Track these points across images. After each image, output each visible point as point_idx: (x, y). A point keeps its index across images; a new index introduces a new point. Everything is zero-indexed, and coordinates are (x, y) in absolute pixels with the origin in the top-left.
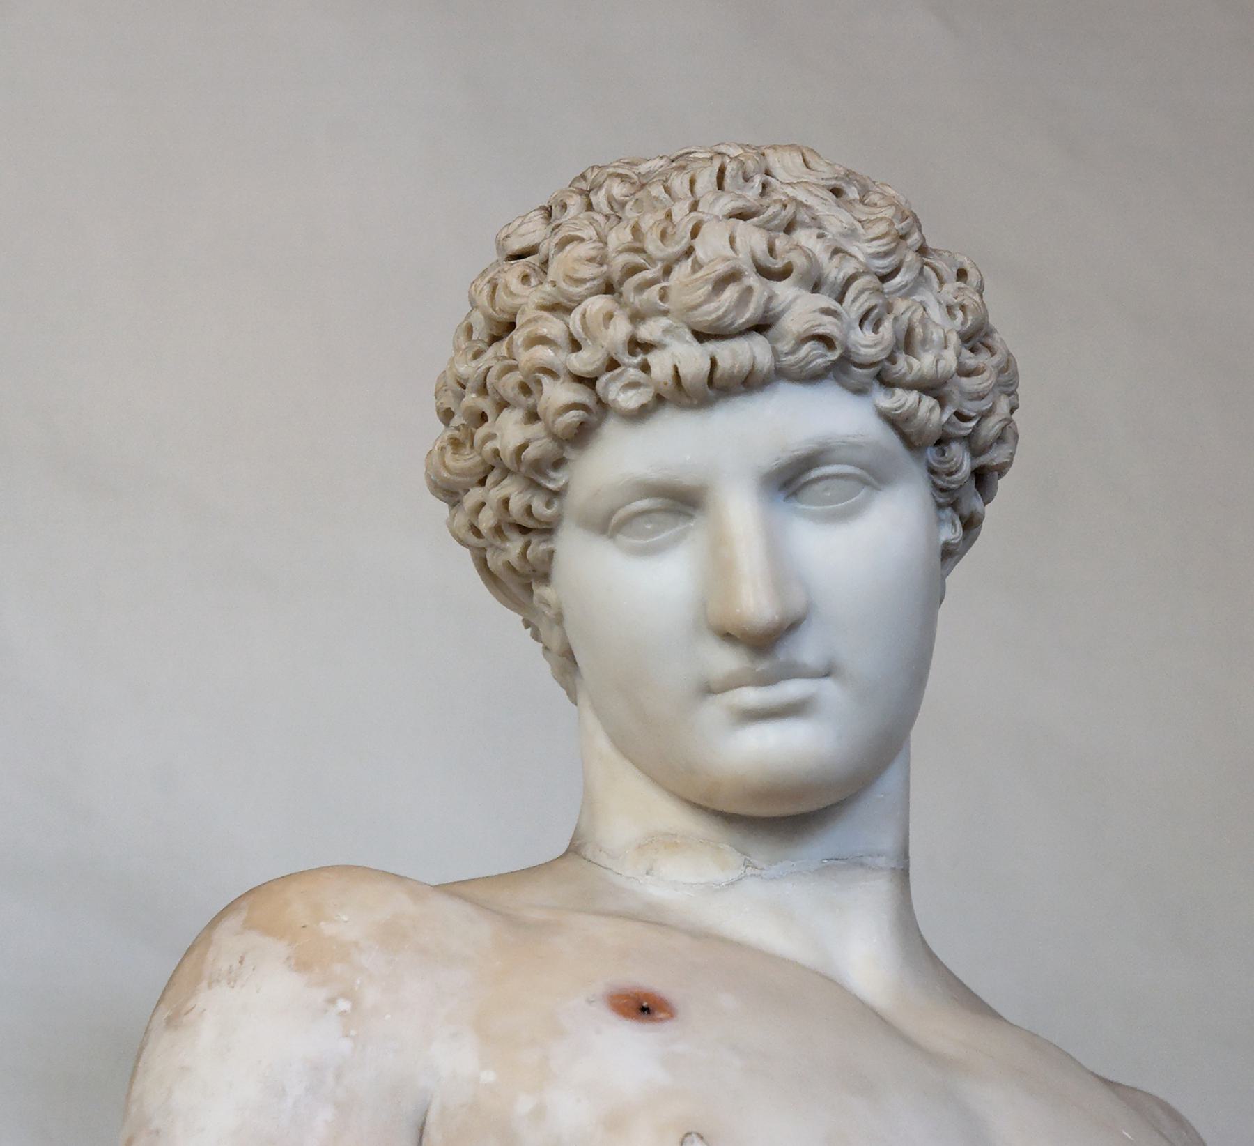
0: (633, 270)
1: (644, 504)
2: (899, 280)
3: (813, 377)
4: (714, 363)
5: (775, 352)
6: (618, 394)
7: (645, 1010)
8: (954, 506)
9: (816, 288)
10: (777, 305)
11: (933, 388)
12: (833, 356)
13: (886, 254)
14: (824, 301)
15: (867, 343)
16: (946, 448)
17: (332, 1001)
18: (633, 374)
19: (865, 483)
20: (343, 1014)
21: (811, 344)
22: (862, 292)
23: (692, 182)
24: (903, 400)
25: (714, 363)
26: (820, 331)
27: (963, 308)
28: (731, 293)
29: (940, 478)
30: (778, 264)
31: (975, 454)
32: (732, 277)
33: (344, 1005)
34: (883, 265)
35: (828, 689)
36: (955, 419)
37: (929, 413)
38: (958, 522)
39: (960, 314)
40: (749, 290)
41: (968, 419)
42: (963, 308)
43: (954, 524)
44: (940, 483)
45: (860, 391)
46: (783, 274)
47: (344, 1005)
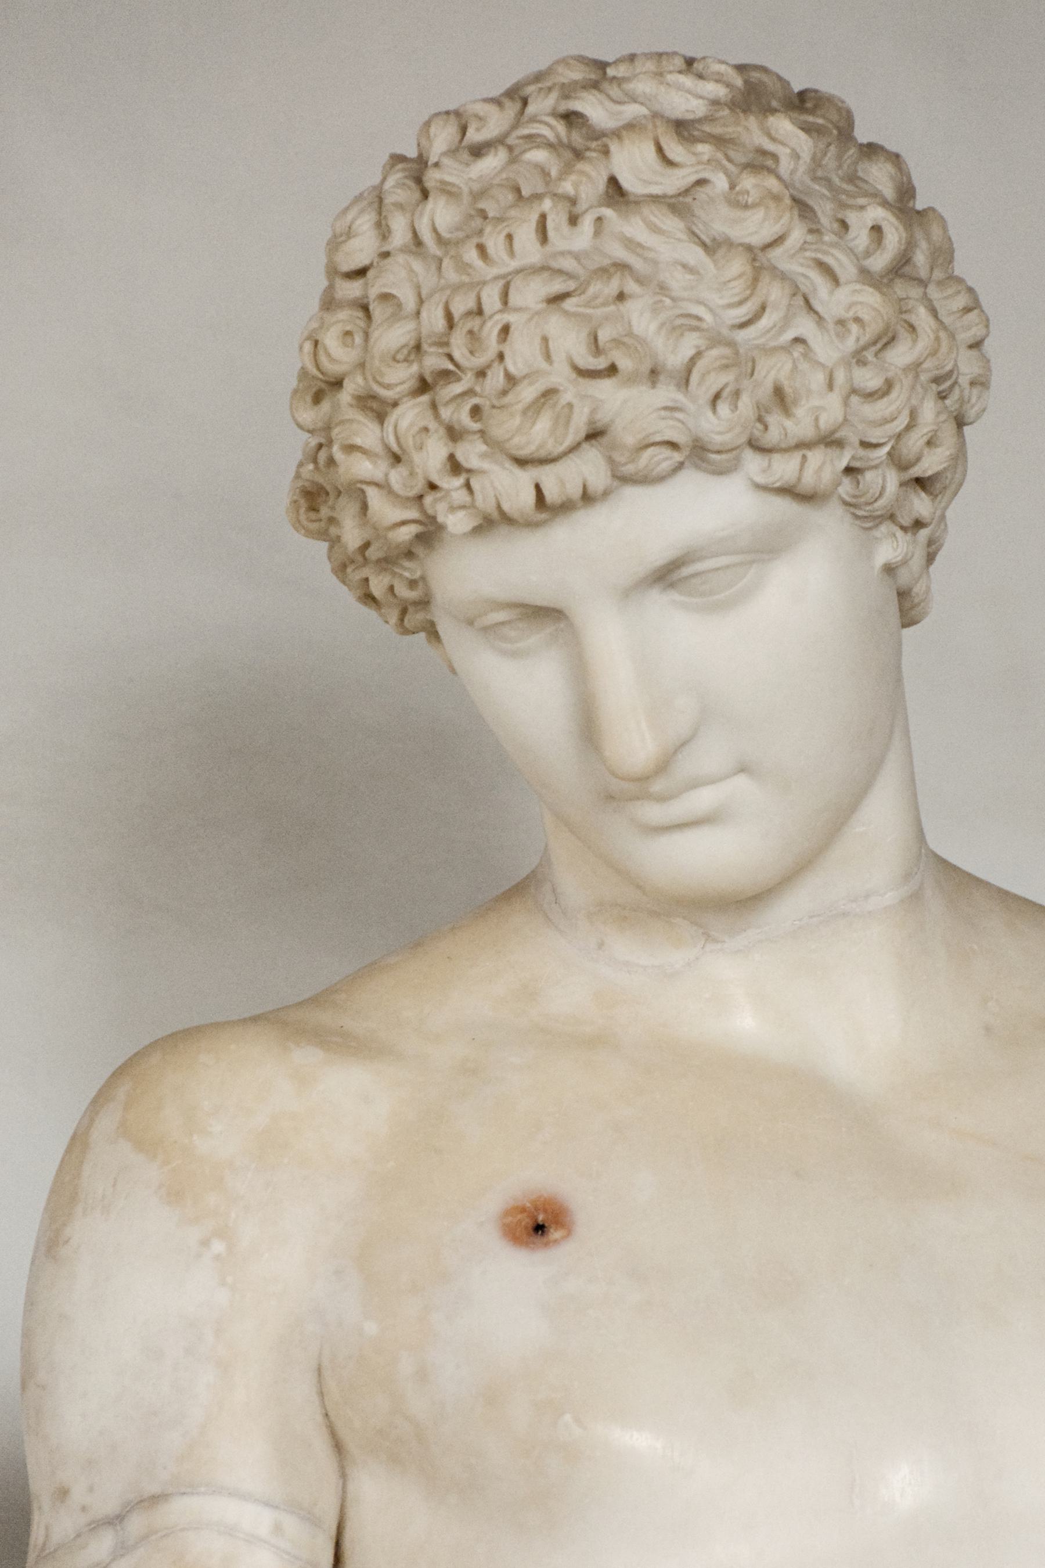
0: (445, 375)
1: (501, 616)
2: (764, 322)
4: (538, 488)
6: (446, 516)
7: (539, 1229)
8: (892, 517)
14: (666, 393)
16: (859, 477)
17: (205, 1243)
18: (460, 496)
19: (752, 562)
20: (217, 1258)
23: (510, 237)
24: (784, 469)
25: (538, 488)
26: (658, 438)
27: (857, 320)
29: (861, 509)
30: (601, 363)
33: (218, 1247)
34: (741, 313)
38: (899, 533)
39: (854, 328)
41: (877, 446)
42: (857, 320)
44: (860, 513)
47: (218, 1247)
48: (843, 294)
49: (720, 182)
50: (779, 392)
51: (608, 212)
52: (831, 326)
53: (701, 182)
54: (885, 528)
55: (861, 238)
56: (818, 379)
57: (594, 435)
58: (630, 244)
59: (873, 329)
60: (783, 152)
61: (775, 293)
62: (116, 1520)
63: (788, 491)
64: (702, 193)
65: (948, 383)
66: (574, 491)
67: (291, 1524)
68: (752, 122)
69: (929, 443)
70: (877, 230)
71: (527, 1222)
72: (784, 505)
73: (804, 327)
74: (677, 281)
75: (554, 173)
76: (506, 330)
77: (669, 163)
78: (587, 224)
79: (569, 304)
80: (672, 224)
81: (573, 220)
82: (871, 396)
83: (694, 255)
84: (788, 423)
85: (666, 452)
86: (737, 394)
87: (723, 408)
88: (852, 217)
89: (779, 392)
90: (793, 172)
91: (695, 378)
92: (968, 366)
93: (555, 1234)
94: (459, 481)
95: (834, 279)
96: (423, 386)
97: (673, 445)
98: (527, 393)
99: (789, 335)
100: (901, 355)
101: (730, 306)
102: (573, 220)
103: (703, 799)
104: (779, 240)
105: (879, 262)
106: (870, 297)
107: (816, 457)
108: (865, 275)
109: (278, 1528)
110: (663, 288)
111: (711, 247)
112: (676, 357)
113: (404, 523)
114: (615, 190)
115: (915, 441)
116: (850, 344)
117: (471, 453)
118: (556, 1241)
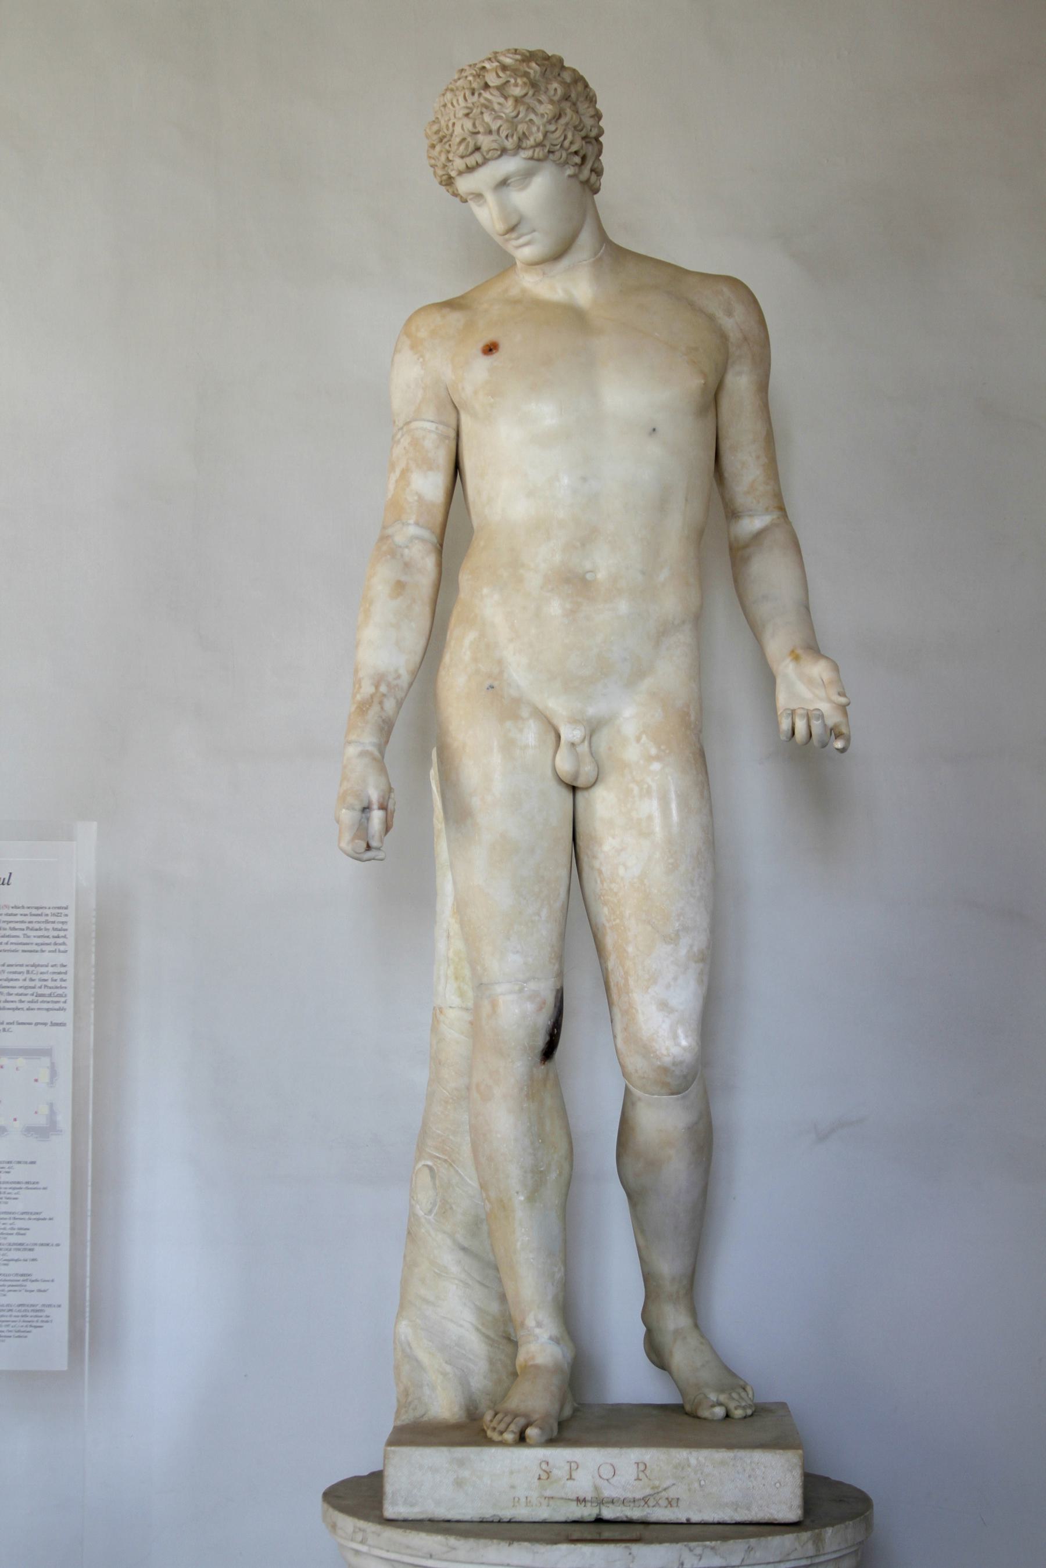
2: (520, 116)
3: (500, 156)
5: (483, 155)
7: (491, 350)
8: (568, 163)
9: (490, 132)
10: (479, 144)
11: (540, 145)
12: (499, 153)
13: (513, 111)
14: (494, 137)
15: (510, 144)
17: (418, 359)
19: (526, 178)
21: (492, 151)
22: (503, 131)
23: (458, 100)
24: (529, 153)
26: (492, 148)
28: (462, 147)
30: (477, 131)
31: (567, 150)
32: (464, 140)
33: (421, 360)
34: (514, 114)
35: (535, 234)
36: (552, 147)
37: (539, 153)
40: (469, 142)
41: (556, 145)
42: (547, 114)
43: (569, 168)
45: (515, 154)
46: (478, 133)
47: (421, 360)
48: (542, 107)
49: (512, 81)
50: (524, 133)
51: (482, 92)
52: (539, 116)
53: (508, 82)
54: (567, 166)
55: (552, 92)
56: (534, 129)
57: (477, 149)
58: (486, 99)
59: (550, 116)
60: (532, 72)
61: (522, 109)
62: (402, 428)
63: (532, 158)
64: (508, 84)
65: (582, 125)
66: (474, 163)
67: (441, 427)
68: (525, 64)
69: (572, 143)
70: (556, 90)
71: (488, 349)
72: (532, 163)
73: (532, 116)
74: (496, 107)
75: (472, 82)
76: (454, 124)
77: (501, 77)
78: (476, 95)
79: (471, 115)
80: (496, 92)
81: (473, 94)
82: (553, 132)
83: (502, 100)
84: (528, 142)
85: (495, 151)
86: (513, 135)
87: (510, 139)
88: (549, 86)
89: (524, 133)
90: (535, 76)
91: (501, 132)
92: (589, 122)
93: (494, 351)
94: (450, 164)
95: (540, 102)
96: (441, 141)
97: (497, 150)
98: (458, 140)
99: (528, 119)
100: (563, 121)
101: (510, 112)
102: (473, 94)
104: (526, 95)
105: (556, 98)
106: (550, 107)
107: (537, 150)
108: (551, 102)
109: (437, 428)
110: (493, 110)
111: (506, 98)
112: (494, 127)
113: (444, 175)
114: (486, 86)
115: (566, 143)
116: (545, 120)
117: (451, 156)
118: (494, 353)
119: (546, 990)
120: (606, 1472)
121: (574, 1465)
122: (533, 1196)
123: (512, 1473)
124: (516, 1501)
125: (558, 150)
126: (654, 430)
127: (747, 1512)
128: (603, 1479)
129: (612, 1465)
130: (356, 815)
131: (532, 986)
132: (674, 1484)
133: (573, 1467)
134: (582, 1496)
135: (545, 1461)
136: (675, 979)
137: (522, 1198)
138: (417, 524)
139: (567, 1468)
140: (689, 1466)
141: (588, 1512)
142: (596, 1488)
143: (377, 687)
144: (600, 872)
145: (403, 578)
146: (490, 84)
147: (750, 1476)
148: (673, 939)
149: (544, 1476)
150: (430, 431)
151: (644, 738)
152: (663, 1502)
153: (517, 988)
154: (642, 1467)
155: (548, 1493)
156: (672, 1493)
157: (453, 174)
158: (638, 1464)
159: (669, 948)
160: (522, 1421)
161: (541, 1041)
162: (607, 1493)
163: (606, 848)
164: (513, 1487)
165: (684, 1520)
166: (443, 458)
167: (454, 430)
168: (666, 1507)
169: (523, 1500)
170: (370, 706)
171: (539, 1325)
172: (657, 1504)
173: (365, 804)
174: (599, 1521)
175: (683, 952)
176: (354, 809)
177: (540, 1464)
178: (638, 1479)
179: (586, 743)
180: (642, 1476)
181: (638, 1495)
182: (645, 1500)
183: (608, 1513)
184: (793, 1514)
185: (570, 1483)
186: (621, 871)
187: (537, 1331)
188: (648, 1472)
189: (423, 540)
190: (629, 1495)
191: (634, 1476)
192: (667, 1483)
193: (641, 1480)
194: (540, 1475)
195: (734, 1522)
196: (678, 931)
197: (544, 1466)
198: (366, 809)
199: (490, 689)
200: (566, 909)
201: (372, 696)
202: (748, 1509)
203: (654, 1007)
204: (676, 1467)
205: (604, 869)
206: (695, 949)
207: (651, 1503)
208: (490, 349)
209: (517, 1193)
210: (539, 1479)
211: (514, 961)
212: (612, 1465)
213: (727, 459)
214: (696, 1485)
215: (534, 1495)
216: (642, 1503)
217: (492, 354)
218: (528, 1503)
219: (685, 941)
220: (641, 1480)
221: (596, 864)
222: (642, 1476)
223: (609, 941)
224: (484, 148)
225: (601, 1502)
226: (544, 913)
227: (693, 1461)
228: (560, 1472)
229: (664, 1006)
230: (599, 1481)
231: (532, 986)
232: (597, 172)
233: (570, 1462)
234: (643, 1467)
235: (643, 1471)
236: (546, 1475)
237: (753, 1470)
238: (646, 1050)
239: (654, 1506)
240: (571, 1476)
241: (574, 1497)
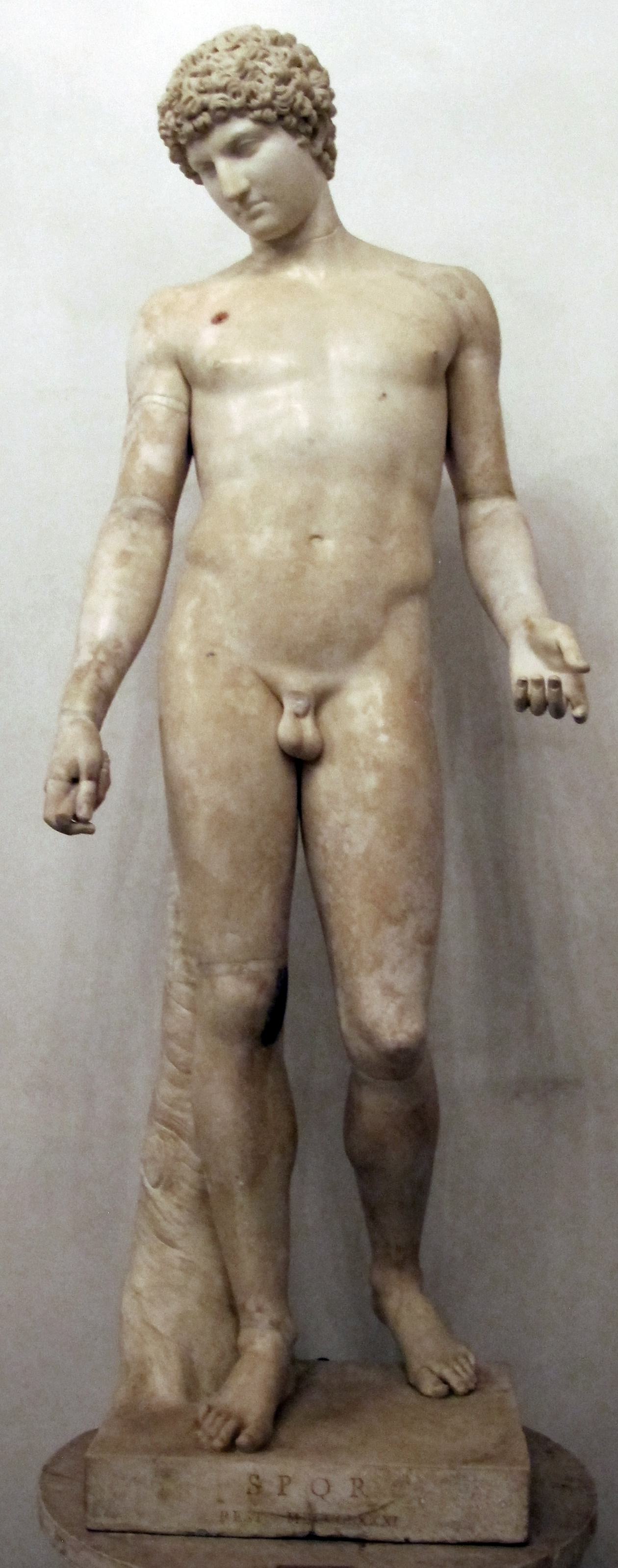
11: (268, 105)
24: (257, 113)
51: (211, 54)
71: (218, 319)
92: (318, 92)
95: (269, 64)
103: (257, 207)
119: (265, 968)
120: (321, 1488)
121: (286, 1480)
122: (254, 1182)
123: (219, 1485)
124: (224, 1516)
125: (287, 114)
126: (384, 395)
127: (469, 1533)
128: (317, 1495)
129: (327, 1481)
130: (62, 784)
131: (253, 966)
132: (392, 1502)
133: (285, 1482)
134: (294, 1510)
135: (254, 1475)
136: (401, 962)
137: (241, 1183)
138: (145, 495)
139: (276, 1482)
140: (408, 1483)
141: (300, 1528)
142: (310, 1505)
143: (95, 653)
144: (325, 850)
145: (130, 548)
146: (219, 48)
147: (473, 1495)
148: (398, 920)
149: (254, 1490)
150: (161, 405)
151: (371, 707)
152: (380, 1521)
153: (236, 968)
154: (358, 1483)
155: (258, 1508)
156: (391, 1511)
157: (182, 141)
158: (353, 1479)
159: (392, 930)
160: (231, 1425)
161: (260, 1023)
162: (321, 1508)
163: (330, 823)
164: (220, 1501)
165: (402, 1539)
166: (173, 431)
167: (185, 404)
168: (383, 1526)
169: (231, 1514)
170: (86, 673)
171: (260, 1310)
172: (374, 1523)
173: (73, 775)
174: (311, 1537)
175: (409, 933)
176: (60, 779)
177: (250, 1478)
178: (354, 1496)
179: (311, 712)
180: (358, 1493)
181: (354, 1512)
182: (361, 1519)
183: (321, 1530)
184: (520, 1537)
185: (281, 1498)
186: (346, 848)
187: (257, 1316)
188: (364, 1489)
189: (151, 511)
190: (344, 1512)
191: (349, 1493)
192: (385, 1501)
193: (357, 1497)
194: (249, 1489)
195: (455, 1542)
196: (405, 911)
197: (254, 1480)
198: (75, 781)
199: (211, 656)
200: (289, 887)
201: (90, 663)
202: (471, 1528)
203: (378, 992)
204: (394, 1485)
205: (328, 846)
206: (422, 931)
207: (368, 1519)
208: (220, 318)
209: (237, 1177)
210: (249, 1493)
211: (232, 940)
212: (327, 1481)
213: (460, 440)
214: (415, 1504)
215: (242, 1509)
216: (358, 1521)
217: (217, 316)
218: (237, 1518)
219: (412, 922)
220: (357, 1497)
221: (321, 840)
222: (358, 1493)
223: (334, 920)
224: (212, 107)
225: (313, 1519)
226: (265, 892)
227: (413, 1479)
228: (271, 1487)
229: (389, 990)
230: (313, 1498)
231: (253, 966)
232: (330, 151)
233: (281, 1477)
234: (358, 1482)
235: (360, 1488)
236: (256, 1488)
237: (477, 1488)
238: (369, 1036)
239: (371, 1524)
240: (282, 1490)
241: (284, 1512)
